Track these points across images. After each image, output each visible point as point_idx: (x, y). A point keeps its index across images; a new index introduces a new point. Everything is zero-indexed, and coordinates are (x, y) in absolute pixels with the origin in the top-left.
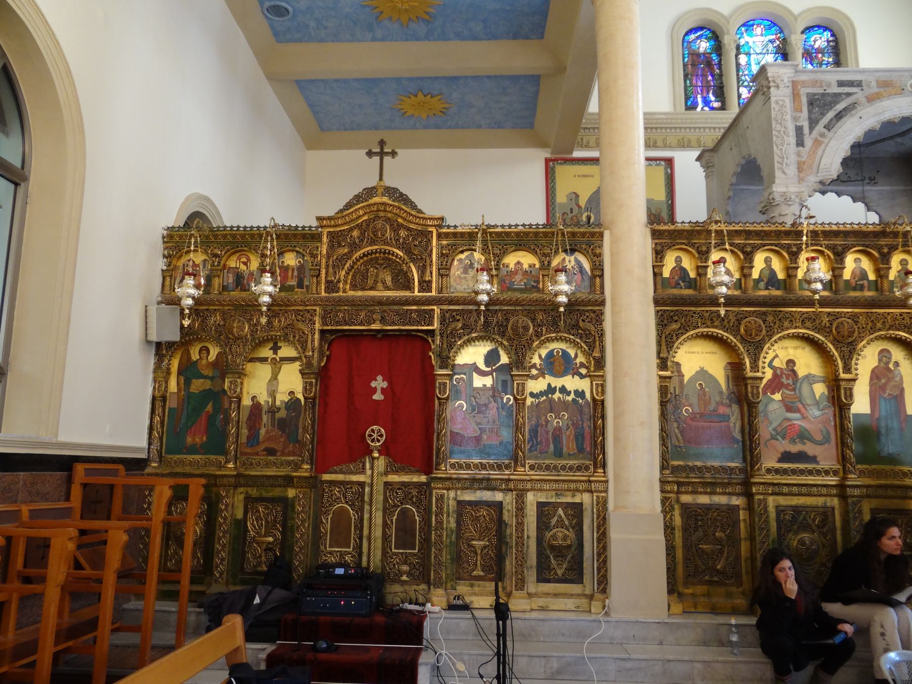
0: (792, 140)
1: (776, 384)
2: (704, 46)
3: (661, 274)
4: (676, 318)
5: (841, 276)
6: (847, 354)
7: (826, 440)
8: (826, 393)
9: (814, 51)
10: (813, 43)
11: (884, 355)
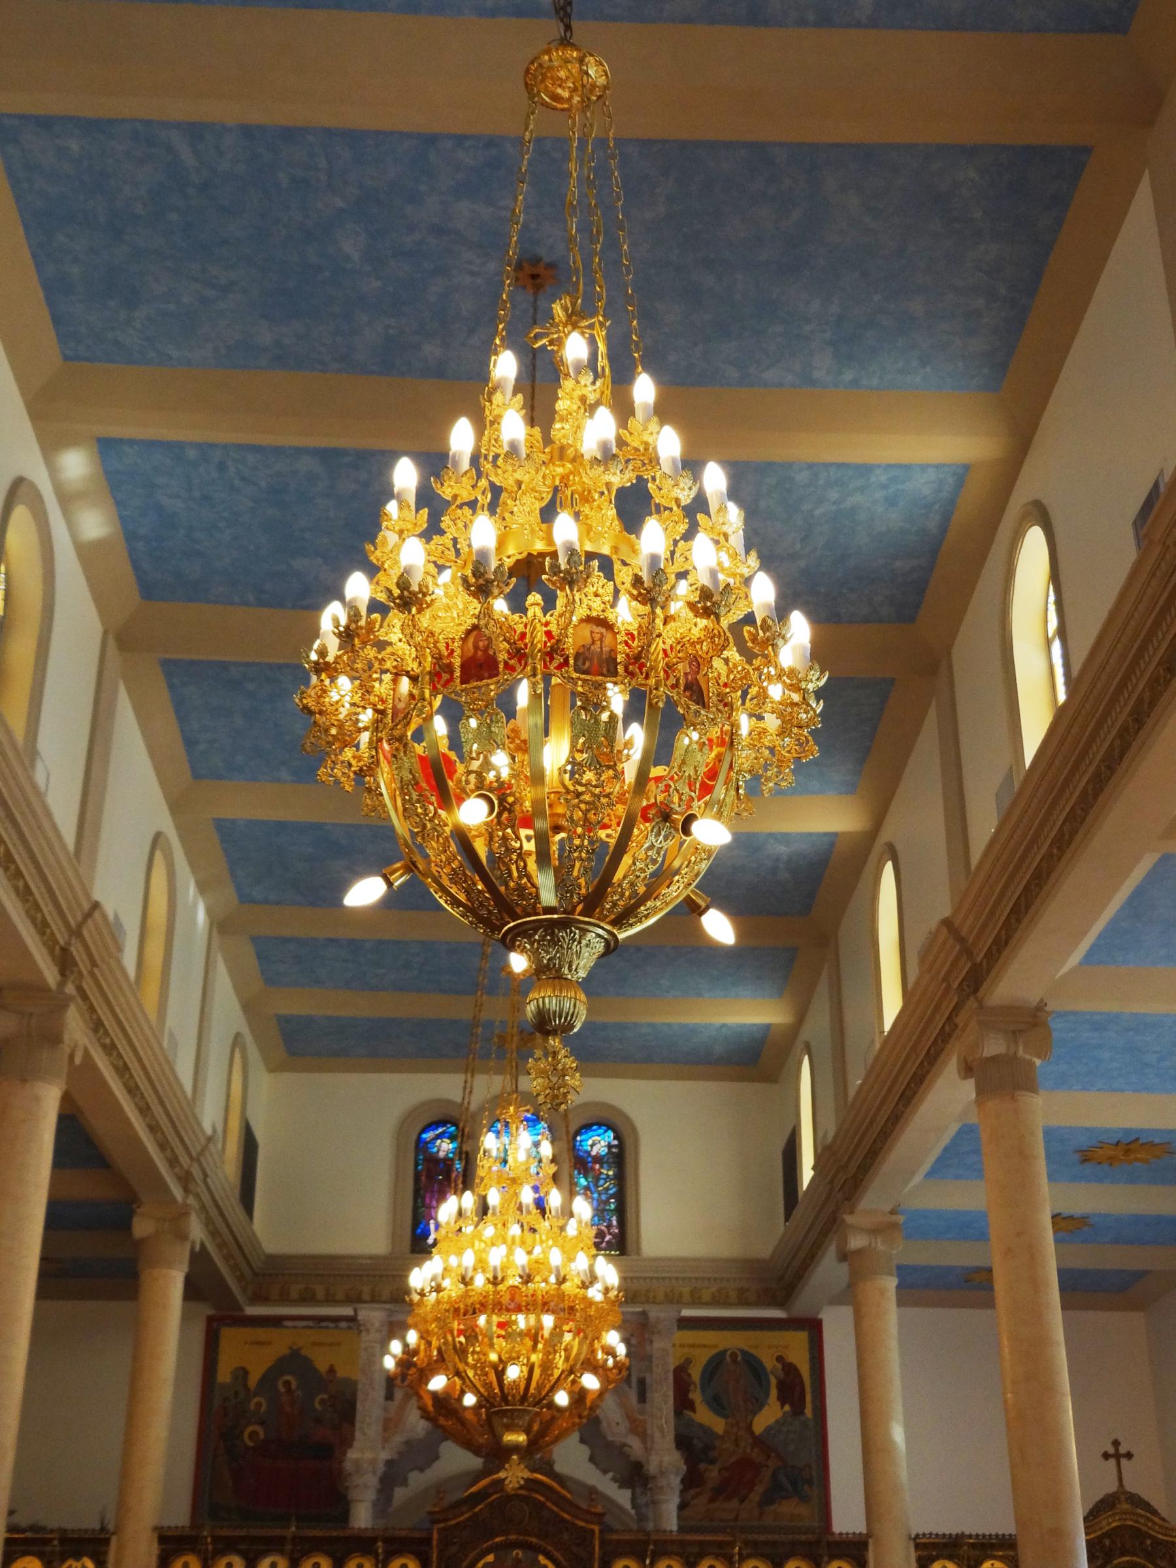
2: (445, 1147)
9: (590, 1159)
10: (589, 1148)
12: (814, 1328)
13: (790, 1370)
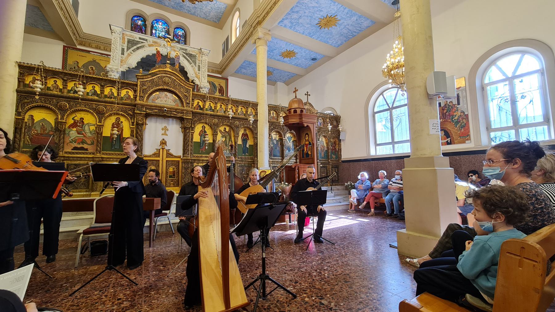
0: (121, 53)
1: (74, 125)
2: (140, 23)
3: (23, 82)
4: (28, 98)
5: (103, 93)
6: (101, 117)
7: (92, 144)
8: (95, 129)
11: (118, 119)
12: (227, 80)
13: (221, 87)
